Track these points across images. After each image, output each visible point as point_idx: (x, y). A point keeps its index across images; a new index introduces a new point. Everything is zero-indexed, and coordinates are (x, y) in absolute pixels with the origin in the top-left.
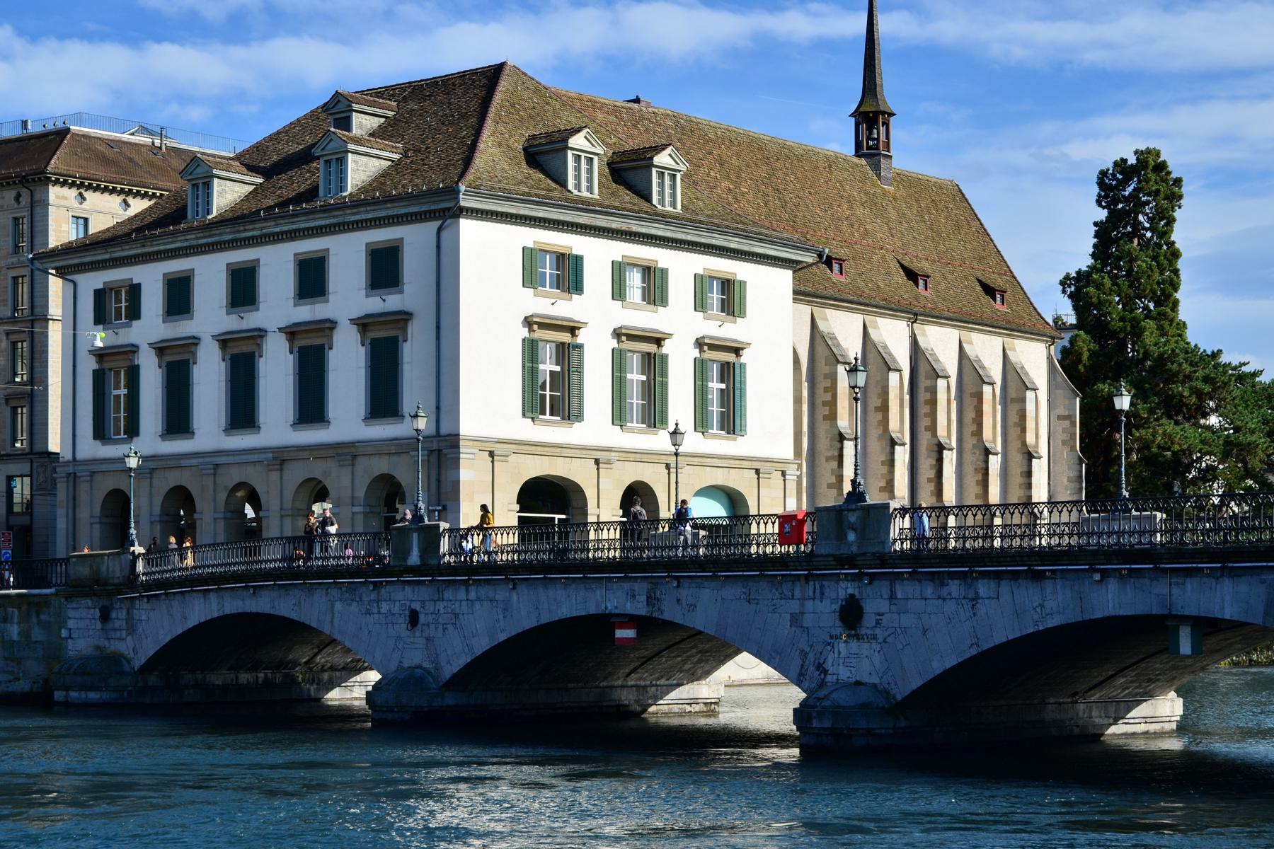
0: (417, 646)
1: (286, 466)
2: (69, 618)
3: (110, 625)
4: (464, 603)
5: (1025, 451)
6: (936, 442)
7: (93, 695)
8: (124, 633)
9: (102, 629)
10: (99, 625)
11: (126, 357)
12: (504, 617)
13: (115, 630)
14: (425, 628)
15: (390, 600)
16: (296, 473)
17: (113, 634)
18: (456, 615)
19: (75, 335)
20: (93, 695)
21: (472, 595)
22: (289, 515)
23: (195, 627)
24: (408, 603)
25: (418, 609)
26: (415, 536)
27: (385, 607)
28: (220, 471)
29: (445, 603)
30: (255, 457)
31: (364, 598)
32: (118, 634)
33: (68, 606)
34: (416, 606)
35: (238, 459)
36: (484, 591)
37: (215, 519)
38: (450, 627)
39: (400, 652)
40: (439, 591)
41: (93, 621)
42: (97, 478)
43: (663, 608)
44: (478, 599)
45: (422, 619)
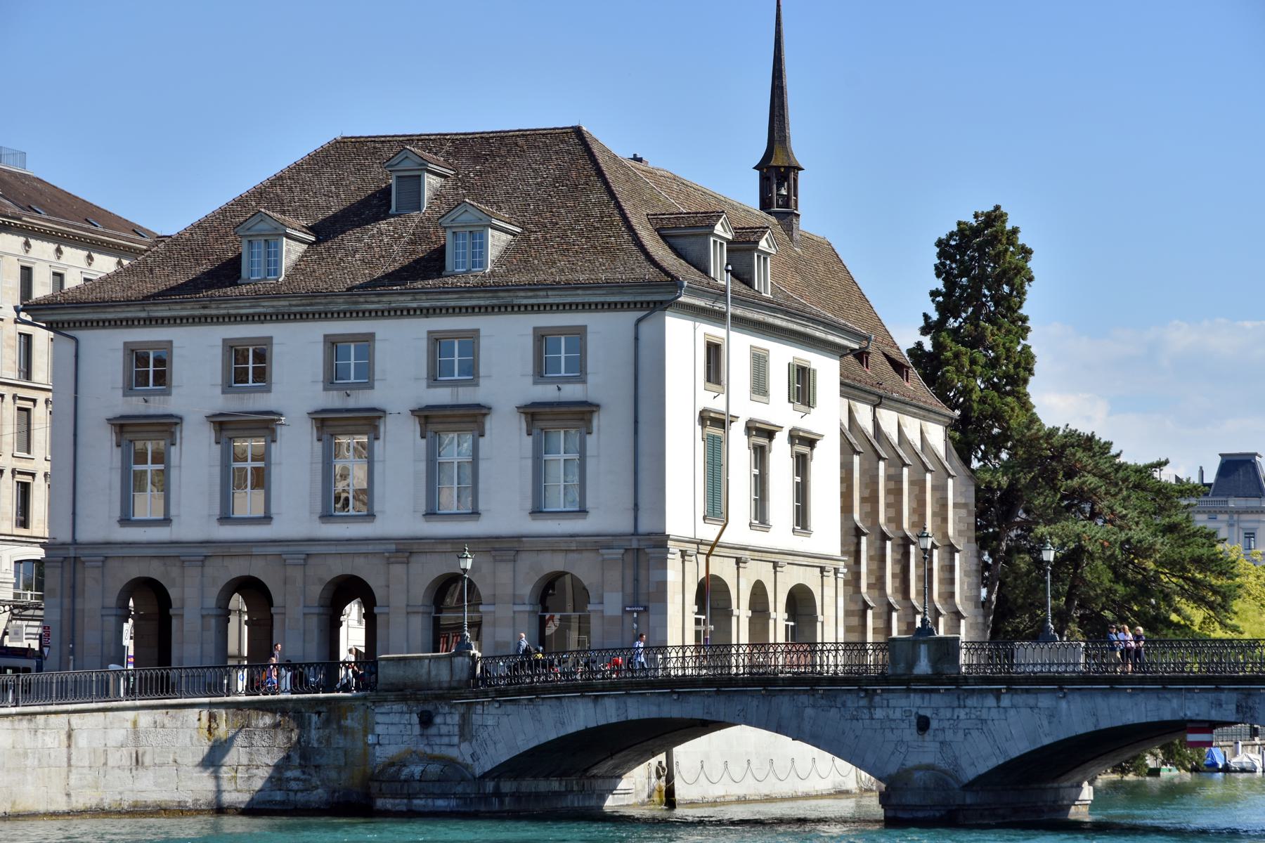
0: (926, 749)
1: (414, 559)
2: (378, 723)
3: (433, 731)
4: (993, 710)
5: (946, 543)
6: (902, 535)
7: (441, 803)
8: (456, 740)
9: (422, 735)
10: (417, 729)
11: (165, 428)
12: (1049, 723)
13: (441, 735)
14: (939, 733)
15: (888, 706)
16: (430, 569)
17: (437, 740)
18: (984, 721)
19: (76, 398)
20: (441, 803)
21: (1006, 701)
22: (418, 613)
23: (578, 733)
24: (914, 710)
25: (929, 715)
26: (923, 650)
27: (879, 713)
28: (311, 561)
29: (967, 710)
30: (370, 548)
31: (849, 704)
32: (446, 740)
33: (376, 711)
34: (928, 713)
35: (341, 549)
36: (1031, 700)
37: (304, 614)
38: (975, 733)
39: (902, 756)
40: (959, 699)
41: (409, 726)
42: (110, 563)
43: (1257, 715)
44: (1013, 706)
45: (934, 724)
